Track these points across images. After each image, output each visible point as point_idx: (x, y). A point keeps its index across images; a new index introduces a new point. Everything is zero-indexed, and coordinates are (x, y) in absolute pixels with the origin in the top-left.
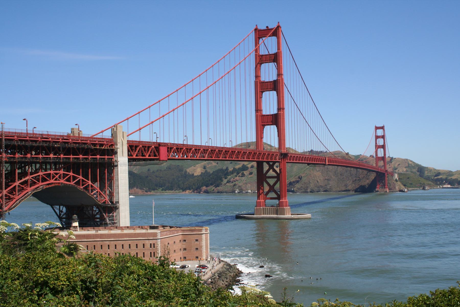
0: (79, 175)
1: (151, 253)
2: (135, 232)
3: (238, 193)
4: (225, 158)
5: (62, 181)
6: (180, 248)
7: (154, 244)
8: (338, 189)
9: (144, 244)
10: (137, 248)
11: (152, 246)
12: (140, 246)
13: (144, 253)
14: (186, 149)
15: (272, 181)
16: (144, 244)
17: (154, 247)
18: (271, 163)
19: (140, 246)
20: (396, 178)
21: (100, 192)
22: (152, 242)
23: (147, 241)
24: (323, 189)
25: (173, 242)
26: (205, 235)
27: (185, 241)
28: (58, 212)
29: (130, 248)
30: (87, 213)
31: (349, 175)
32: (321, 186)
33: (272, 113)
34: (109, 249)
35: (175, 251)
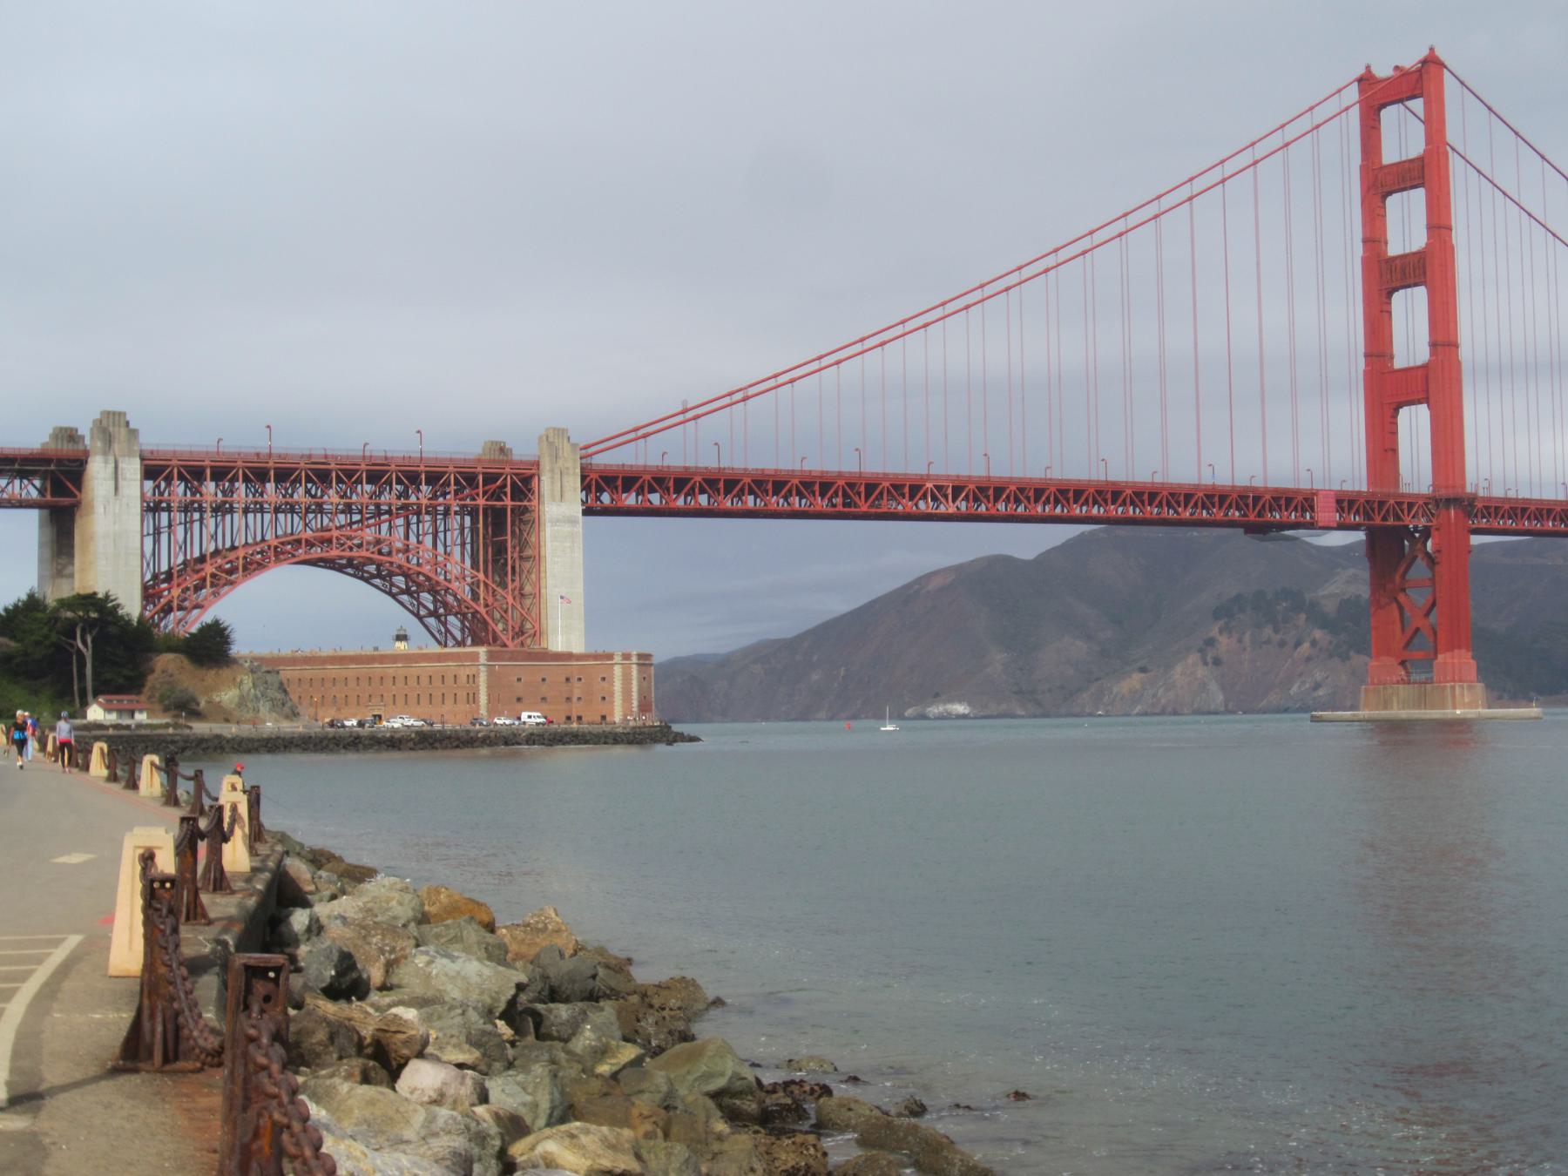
1: (468, 694)
10: (443, 683)
11: (471, 680)
13: (455, 694)
22: (468, 671)
23: (462, 668)
27: (580, 679)
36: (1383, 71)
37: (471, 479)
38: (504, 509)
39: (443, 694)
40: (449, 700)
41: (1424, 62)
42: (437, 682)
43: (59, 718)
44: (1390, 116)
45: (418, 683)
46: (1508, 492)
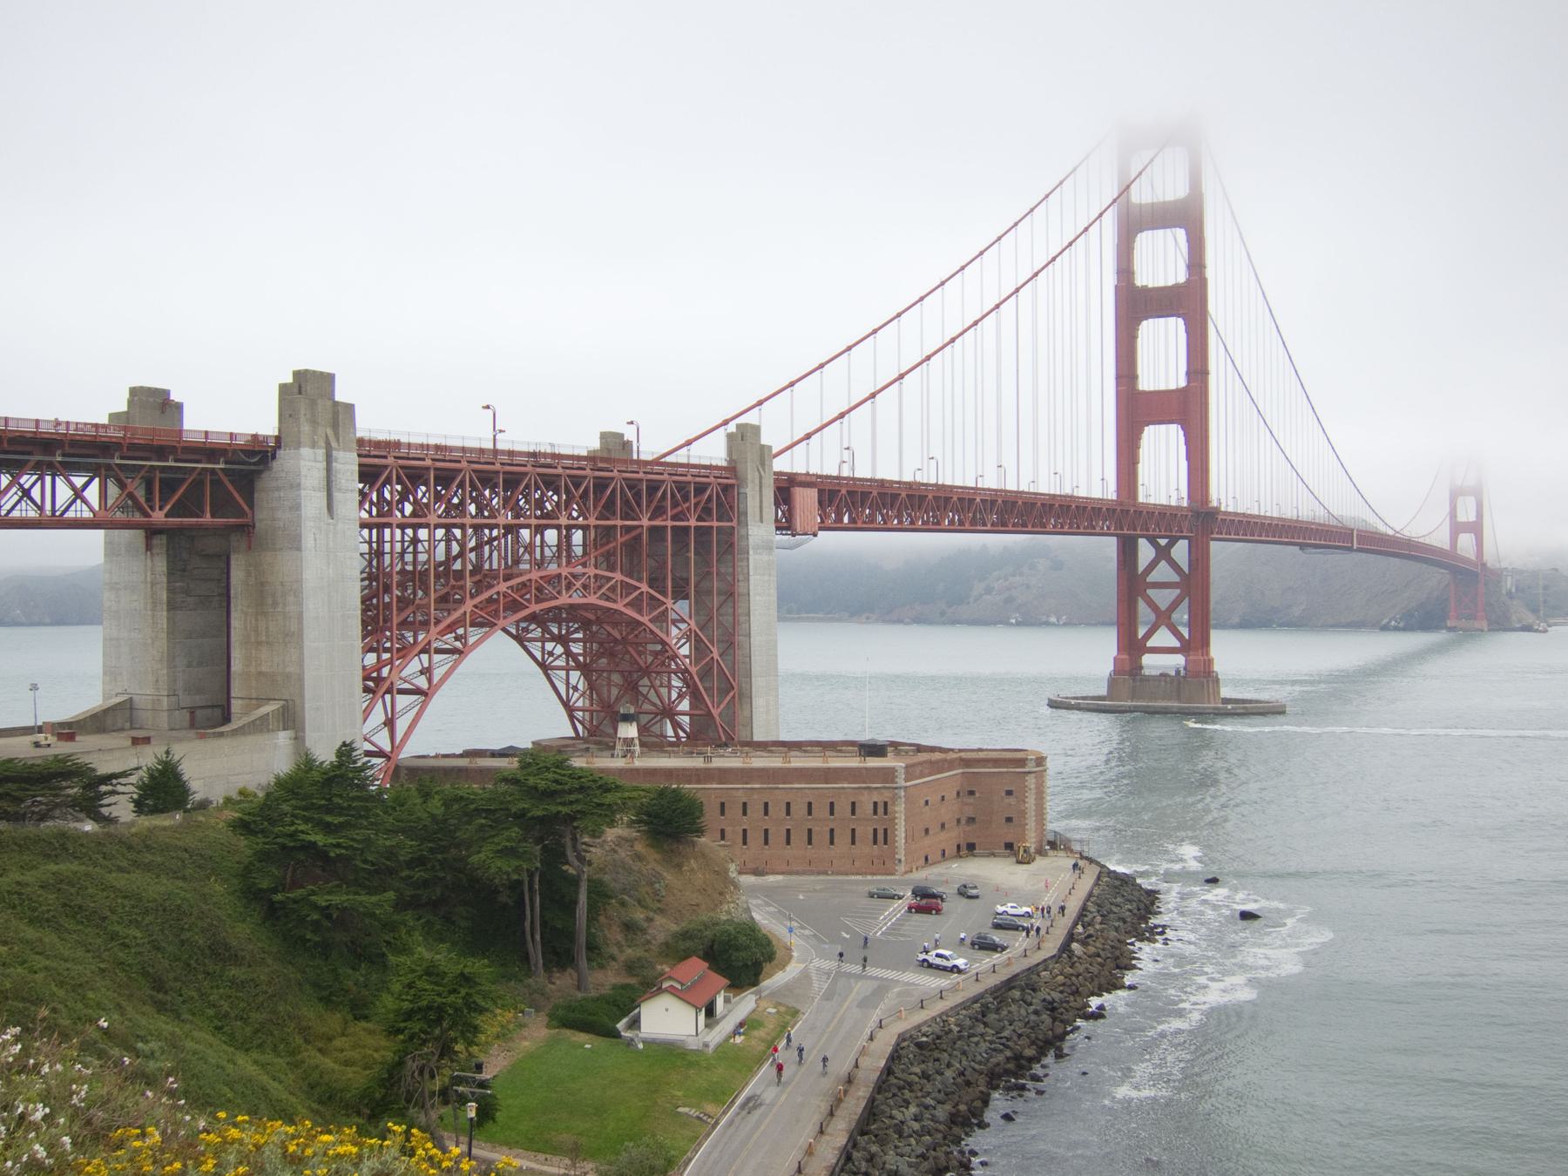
0: (640, 580)
1: (875, 831)
2: (825, 765)
4: (1023, 526)
5: (592, 599)
6: (957, 817)
7: (886, 804)
9: (853, 804)
10: (832, 813)
11: (881, 810)
12: (843, 808)
13: (853, 830)
14: (907, 495)
15: (1163, 598)
16: (853, 804)
17: (886, 813)
18: (1163, 542)
19: (843, 808)
20: (1509, 587)
21: (696, 635)
23: (865, 792)
25: (940, 798)
26: (1036, 777)
27: (972, 793)
28: (562, 688)
29: (810, 813)
30: (652, 696)
33: (1173, 386)
34: (745, 813)
35: (943, 826)
39: (832, 831)
40: (843, 839)
42: (821, 811)
43: (996, 1088)
45: (788, 813)
46: (980, 479)
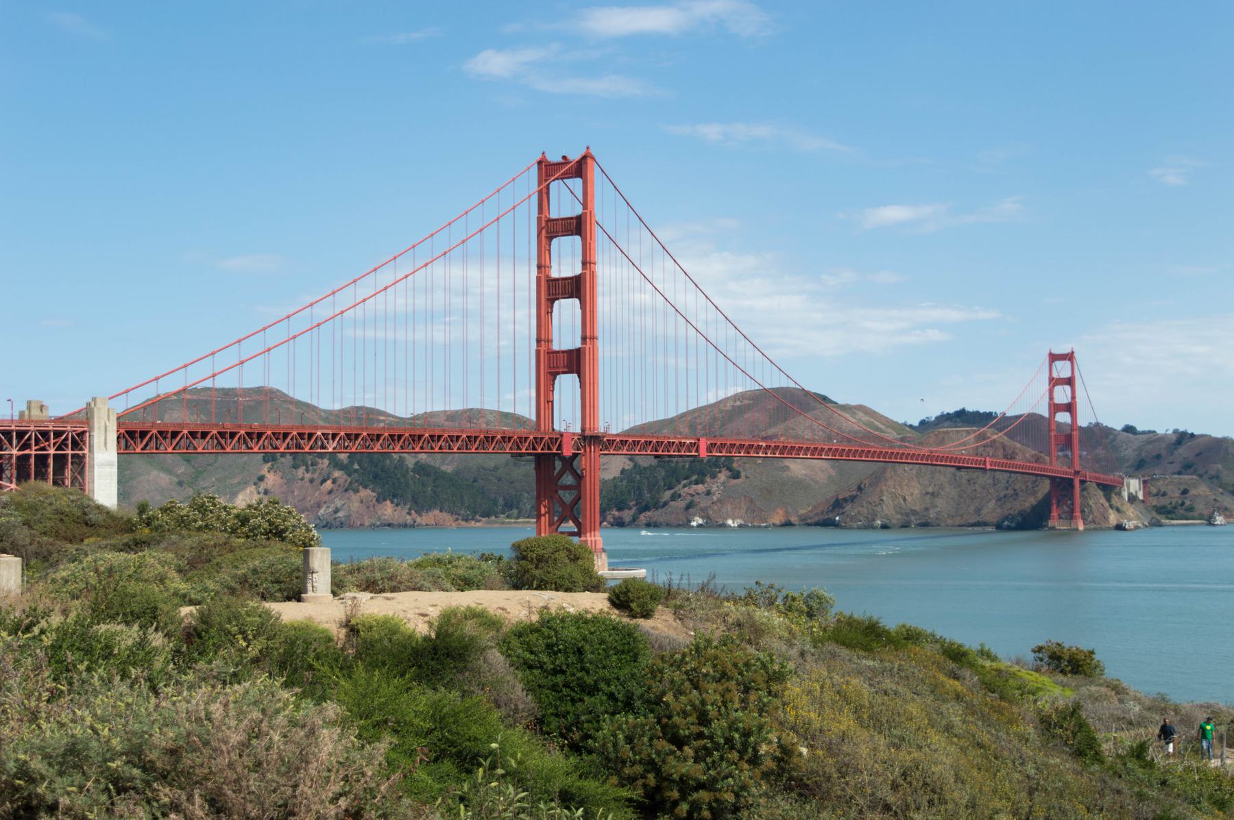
3: (700, 526)
8: (958, 521)
24: (920, 519)
31: (991, 481)
32: (914, 512)
36: (554, 158)
37: (45, 434)
38: (73, 456)
41: (584, 158)
44: (556, 187)
